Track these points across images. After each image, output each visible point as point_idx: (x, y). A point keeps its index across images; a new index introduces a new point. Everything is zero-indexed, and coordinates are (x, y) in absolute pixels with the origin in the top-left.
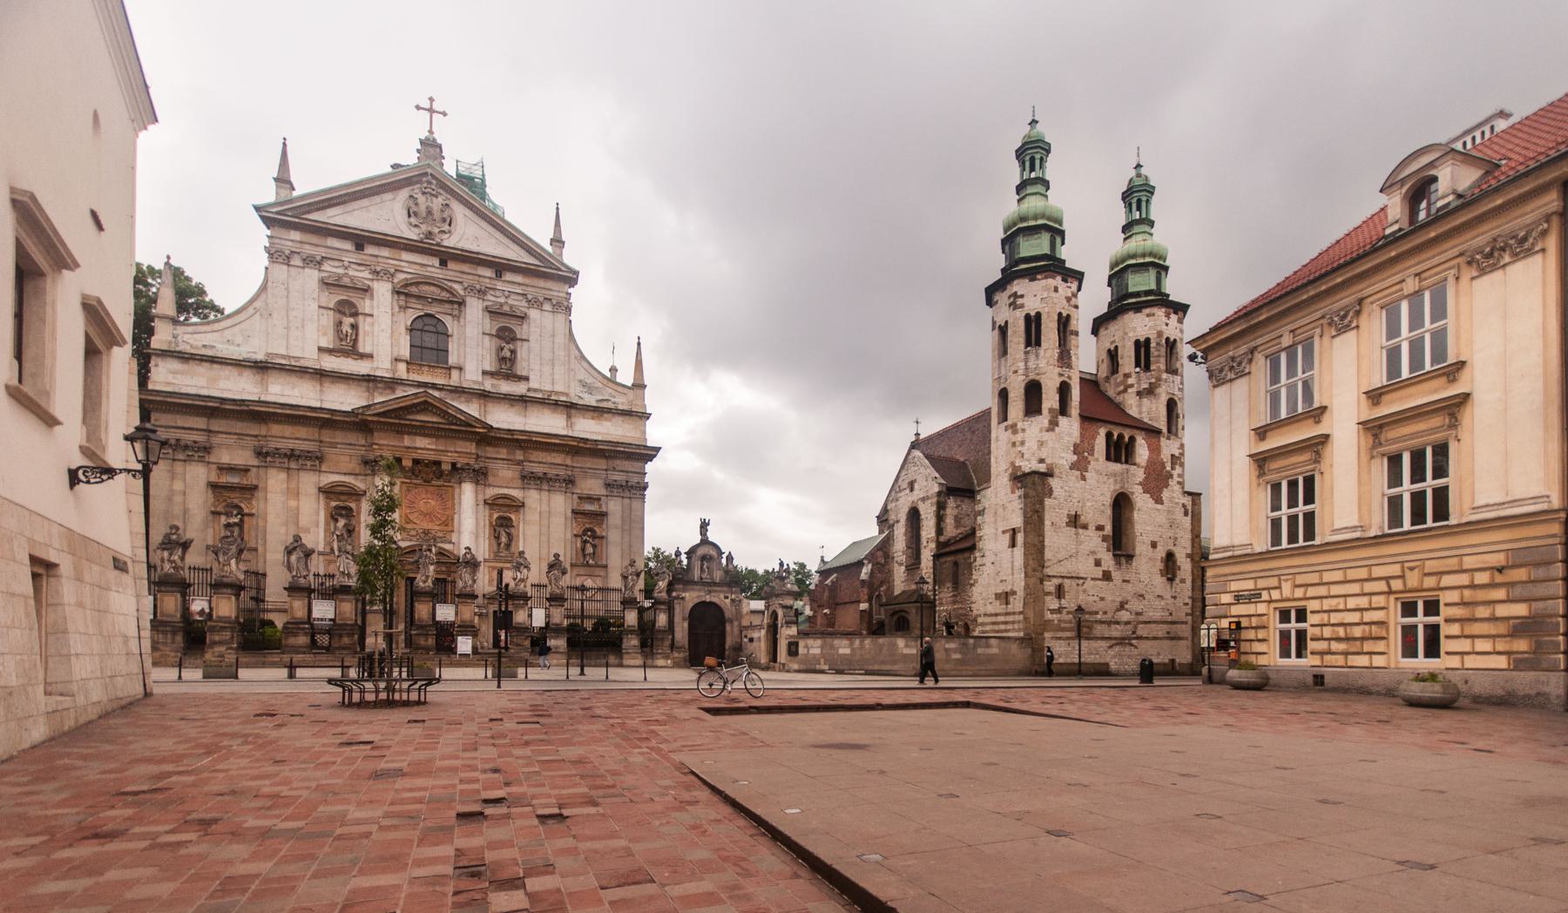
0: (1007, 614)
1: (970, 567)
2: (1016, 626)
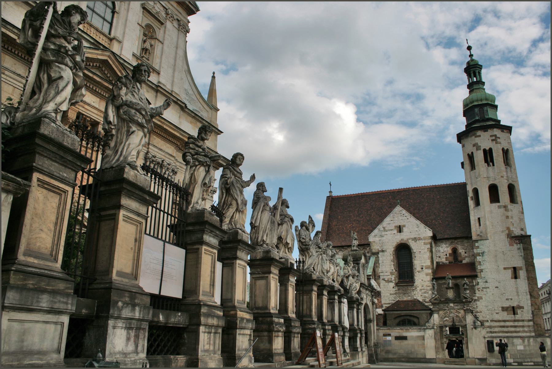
0: (515, 321)
1: (473, 289)
2: (526, 329)
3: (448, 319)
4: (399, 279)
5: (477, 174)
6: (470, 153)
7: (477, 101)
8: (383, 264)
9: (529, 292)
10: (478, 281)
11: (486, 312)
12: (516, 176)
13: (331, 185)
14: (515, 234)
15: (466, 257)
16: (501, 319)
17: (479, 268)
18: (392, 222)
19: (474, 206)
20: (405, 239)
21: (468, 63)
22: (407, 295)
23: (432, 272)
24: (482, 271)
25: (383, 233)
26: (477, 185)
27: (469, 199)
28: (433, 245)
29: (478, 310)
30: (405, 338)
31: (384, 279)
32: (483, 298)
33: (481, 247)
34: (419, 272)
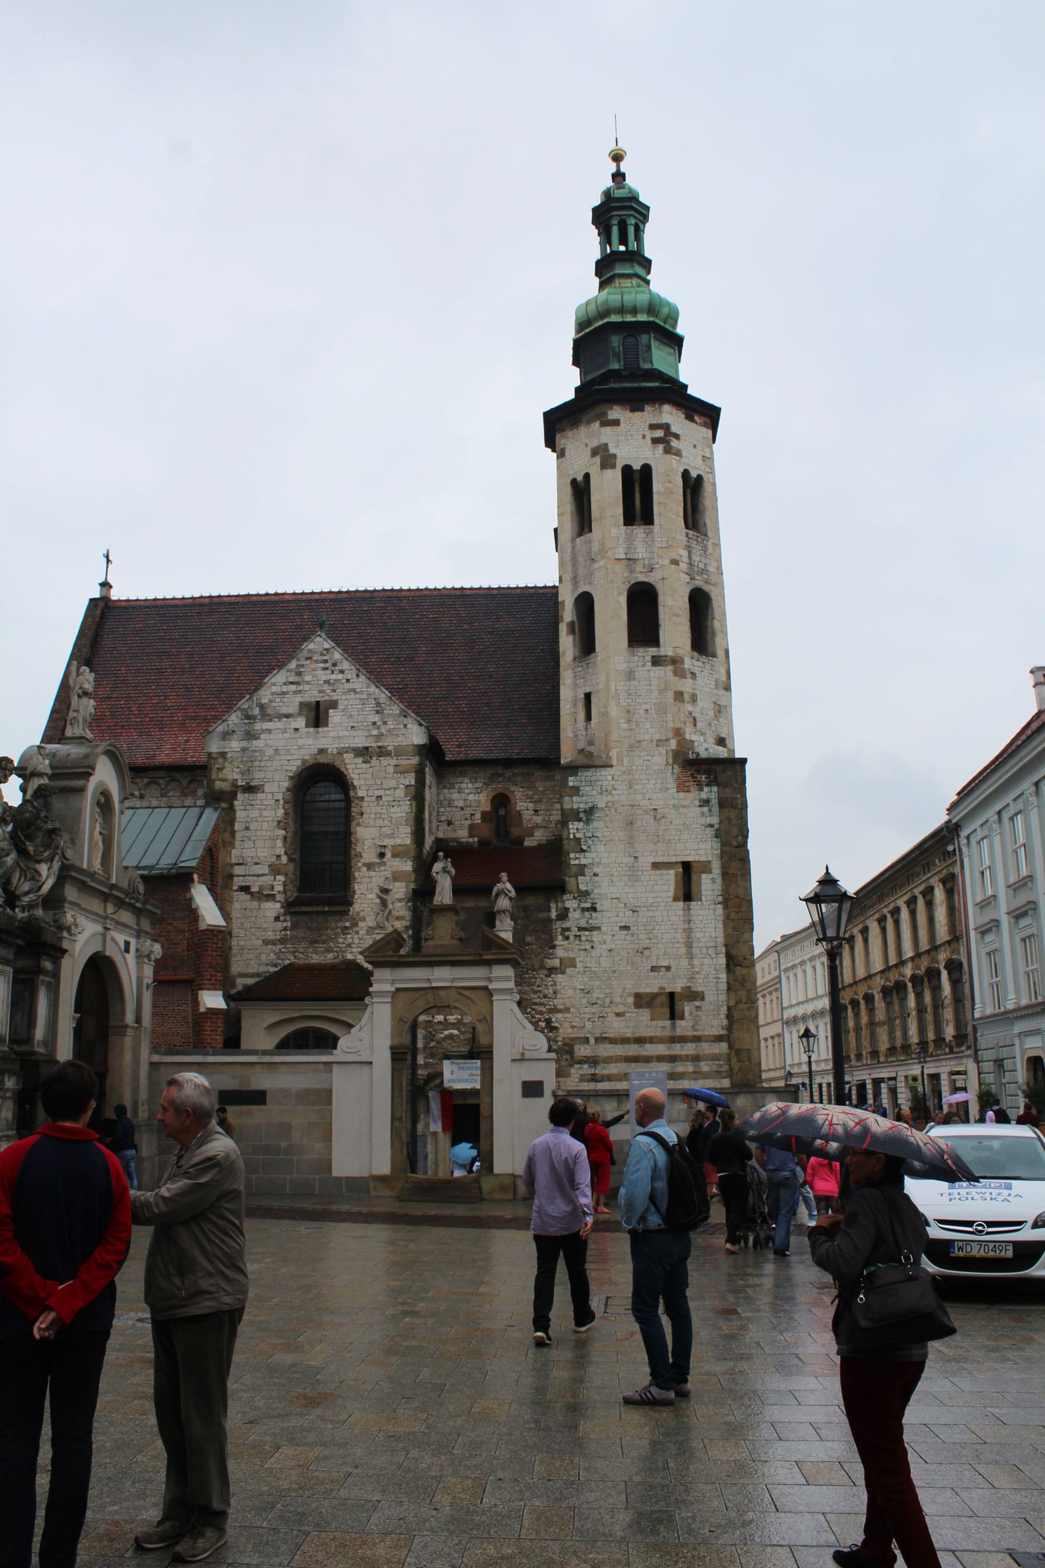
2: (705, 1067)
3: (455, 1032)
4: (301, 889)
5: (595, 548)
6: (580, 478)
7: (621, 310)
8: (248, 833)
9: (726, 945)
10: (568, 904)
11: (583, 1010)
12: (719, 568)
13: (108, 561)
14: (698, 754)
15: (537, 826)
16: (629, 1035)
17: (572, 862)
18: (293, 688)
19: (577, 653)
20: (333, 747)
21: (607, 194)
22: (321, 947)
23: (414, 871)
24: (581, 870)
25: (258, 726)
26: (590, 583)
27: (563, 628)
28: (429, 778)
29: (559, 1003)
30: (258, 1097)
31: (245, 889)
32: (579, 965)
33: (585, 789)
34: (370, 866)
